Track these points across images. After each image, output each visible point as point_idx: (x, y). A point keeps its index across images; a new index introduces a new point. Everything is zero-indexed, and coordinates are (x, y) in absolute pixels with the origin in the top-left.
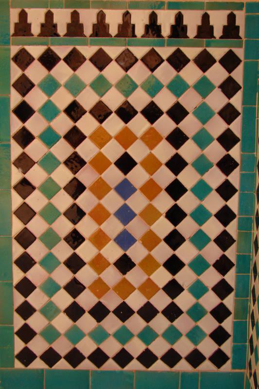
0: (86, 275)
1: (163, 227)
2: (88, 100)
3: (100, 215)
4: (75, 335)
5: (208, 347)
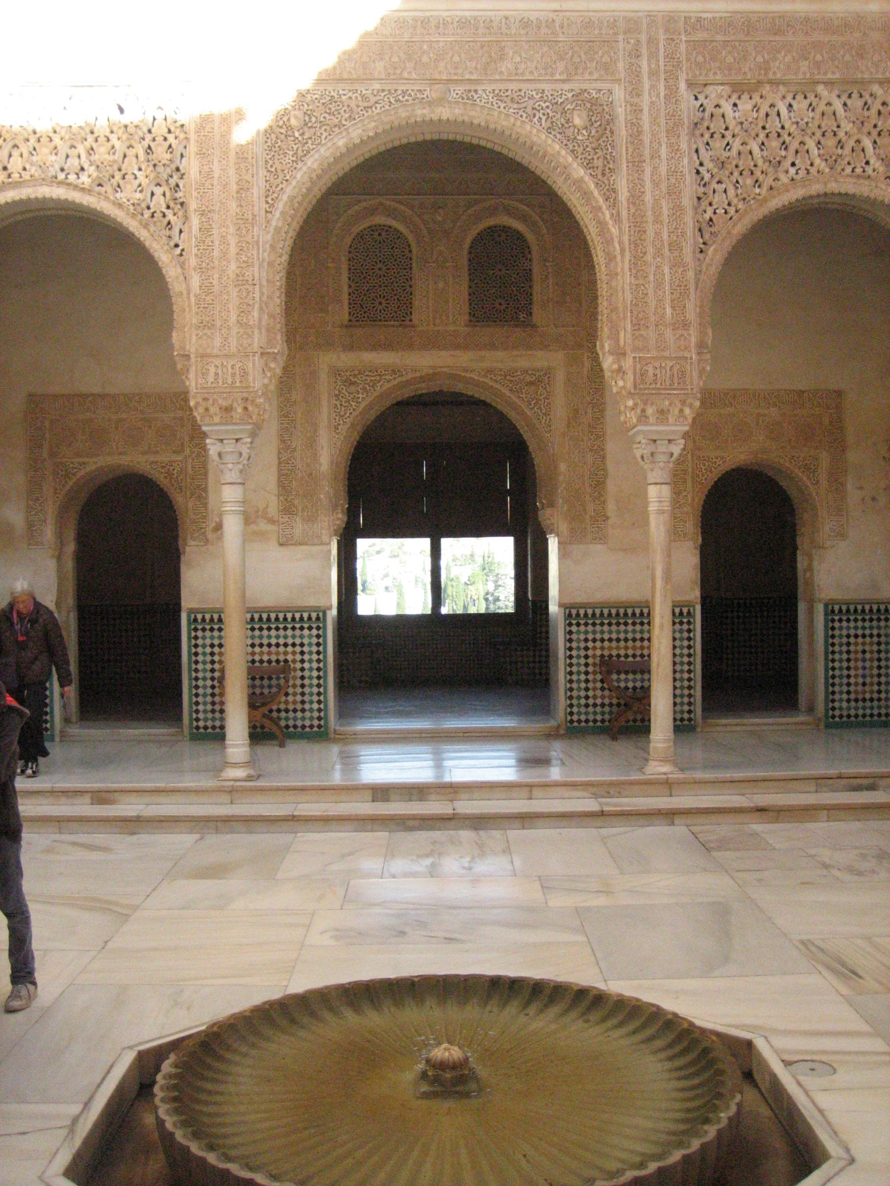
0: (852, 688)
2: (852, 632)
3: (856, 668)
4: (849, 709)
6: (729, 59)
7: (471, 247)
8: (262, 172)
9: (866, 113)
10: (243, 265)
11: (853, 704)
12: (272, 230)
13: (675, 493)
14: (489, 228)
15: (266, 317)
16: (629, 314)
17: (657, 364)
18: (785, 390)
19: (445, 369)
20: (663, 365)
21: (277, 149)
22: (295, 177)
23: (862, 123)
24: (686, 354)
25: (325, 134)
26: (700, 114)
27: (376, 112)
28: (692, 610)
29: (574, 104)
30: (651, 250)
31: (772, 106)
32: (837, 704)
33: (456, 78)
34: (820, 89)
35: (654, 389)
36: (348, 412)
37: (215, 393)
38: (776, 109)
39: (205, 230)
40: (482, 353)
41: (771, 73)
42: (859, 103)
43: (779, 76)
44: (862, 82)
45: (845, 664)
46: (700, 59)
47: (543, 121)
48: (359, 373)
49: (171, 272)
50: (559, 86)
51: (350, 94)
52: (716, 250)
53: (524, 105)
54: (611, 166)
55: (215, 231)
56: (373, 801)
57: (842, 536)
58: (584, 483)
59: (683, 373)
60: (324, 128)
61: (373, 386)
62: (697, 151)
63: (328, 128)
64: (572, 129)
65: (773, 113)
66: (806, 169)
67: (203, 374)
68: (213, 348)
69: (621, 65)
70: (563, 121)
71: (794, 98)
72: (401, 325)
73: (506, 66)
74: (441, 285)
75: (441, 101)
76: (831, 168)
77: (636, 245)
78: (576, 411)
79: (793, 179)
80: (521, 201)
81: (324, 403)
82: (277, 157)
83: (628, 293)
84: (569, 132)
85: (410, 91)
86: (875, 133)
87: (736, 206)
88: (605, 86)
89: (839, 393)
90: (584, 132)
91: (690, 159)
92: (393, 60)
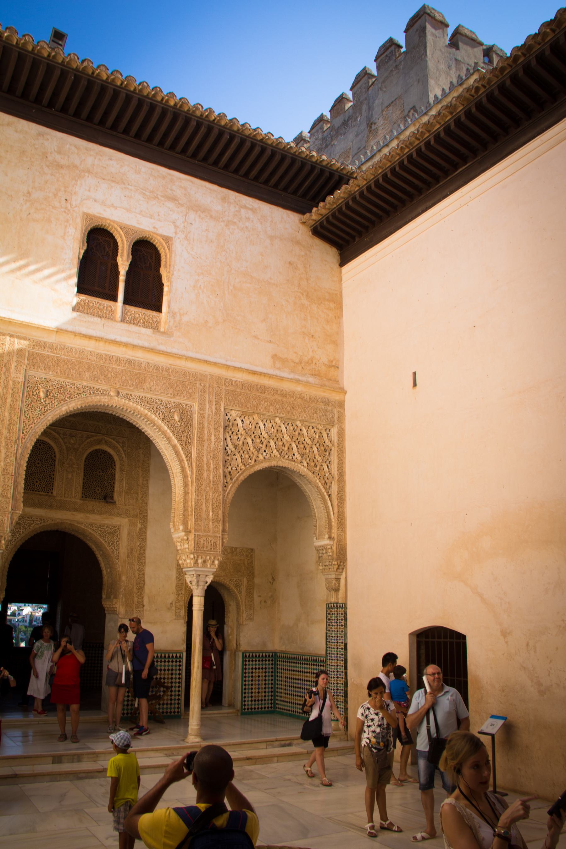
1: (264, 686)
4: (252, 705)
5: (270, 706)
6: (242, 400)
7: (86, 459)
11: (253, 702)
13: (177, 595)
14: (96, 450)
16: (193, 513)
17: (204, 538)
18: (229, 547)
21: (31, 406)
24: (217, 535)
26: (228, 423)
28: (181, 655)
30: (205, 483)
31: (257, 423)
32: (246, 703)
34: (277, 420)
35: (203, 550)
36: (14, 539)
40: (88, 515)
42: (292, 428)
45: (250, 683)
46: (230, 398)
47: (161, 415)
51: (71, 386)
52: (232, 487)
53: (153, 406)
56: (53, 763)
57: (251, 619)
58: (133, 587)
59: (215, 544)
60: (56, 400)
61: (29, 526)
62: (226, 439)
64: (173, 421)
65: (258, 427)
69: (197, 395)
72: (46, 495)
76: (280, 455)
77: (199, 481)
78: (132, 550)
80: (114, 439)
82: (30, 410)
83: (194, 503)
84: (172, 422)
85: (100, 390)
86: (297, 442)
89: (252, 550)
90: (179, 423)
92: (94, 373)
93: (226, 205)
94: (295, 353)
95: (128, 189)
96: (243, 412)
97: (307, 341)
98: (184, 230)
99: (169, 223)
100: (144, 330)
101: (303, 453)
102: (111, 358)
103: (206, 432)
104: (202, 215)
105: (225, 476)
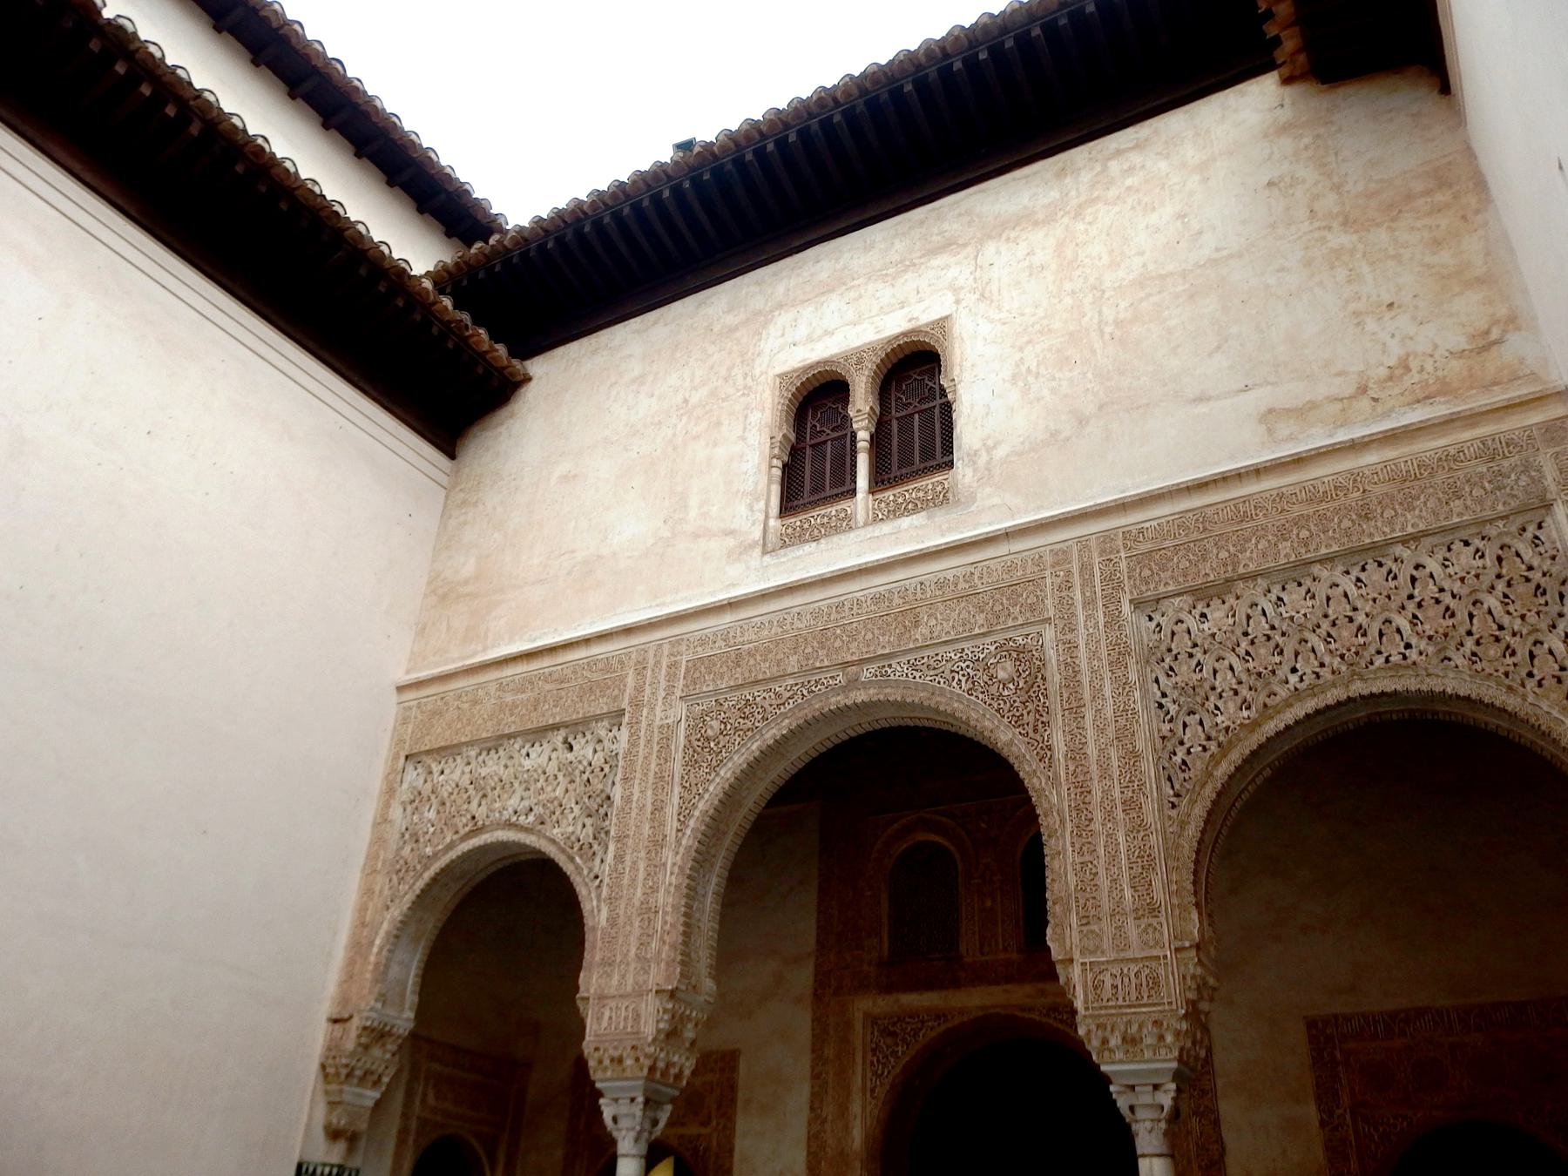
8: (677, 789)
9: (1392, 584)
10: (649, 891)
12: (682, 850)
15: (667, 947)
19: (998, 1010)
20: (1125, 971)
22: (707, 790)
23: (1389, 597)
24: (1155, 952)
25: (738, 739)
26: (1156, 637)
27: (788, 707)
29: (999, 656)
30: (1098, 815)
33: (868, 656)
37: (606, 1041)
38: (1260, 608)
39: (619, 858)
40: (1040, 985)
41: (1241, 566)
43: (1252, 567)
44: (1374, 547)
46: (1146, 573)
48: (899, 1020)
49: (586, 907)
50: (979, 642)
53: (941, 670)
54: (1044, 719)
55: (628, 858)
59: (1155, 983)
61: (914, 1036)
62: (1157, 681)
63: (741, 733)
66: (1314, 673)
67: (598, 1019)
68: (610, 987)
69: (1048, 602)
70: (986, 678)
71: (1284, 589)
73: (923, 630)
74: (989, 903)
75: (853, 683)
79: (1296, 689)
81: (859, 1060)
84: (993, 690)
86: (1411, 607)
87: (1217, 738)
88: (1033, 630)
90: (1011, 686)
91: (1145, 694)
93: (1068, 180)
94: (1339, 374)
95: (853, 287)
96: (1192, 591)
97: (1371, 325)
98: (975, 286)
99: (940, 294)
100: (905, 522)
101: (1441, 631)
102: (839, 607)
103: (1085, 680)
104: (1013, 235)
105: (1170, 779)
